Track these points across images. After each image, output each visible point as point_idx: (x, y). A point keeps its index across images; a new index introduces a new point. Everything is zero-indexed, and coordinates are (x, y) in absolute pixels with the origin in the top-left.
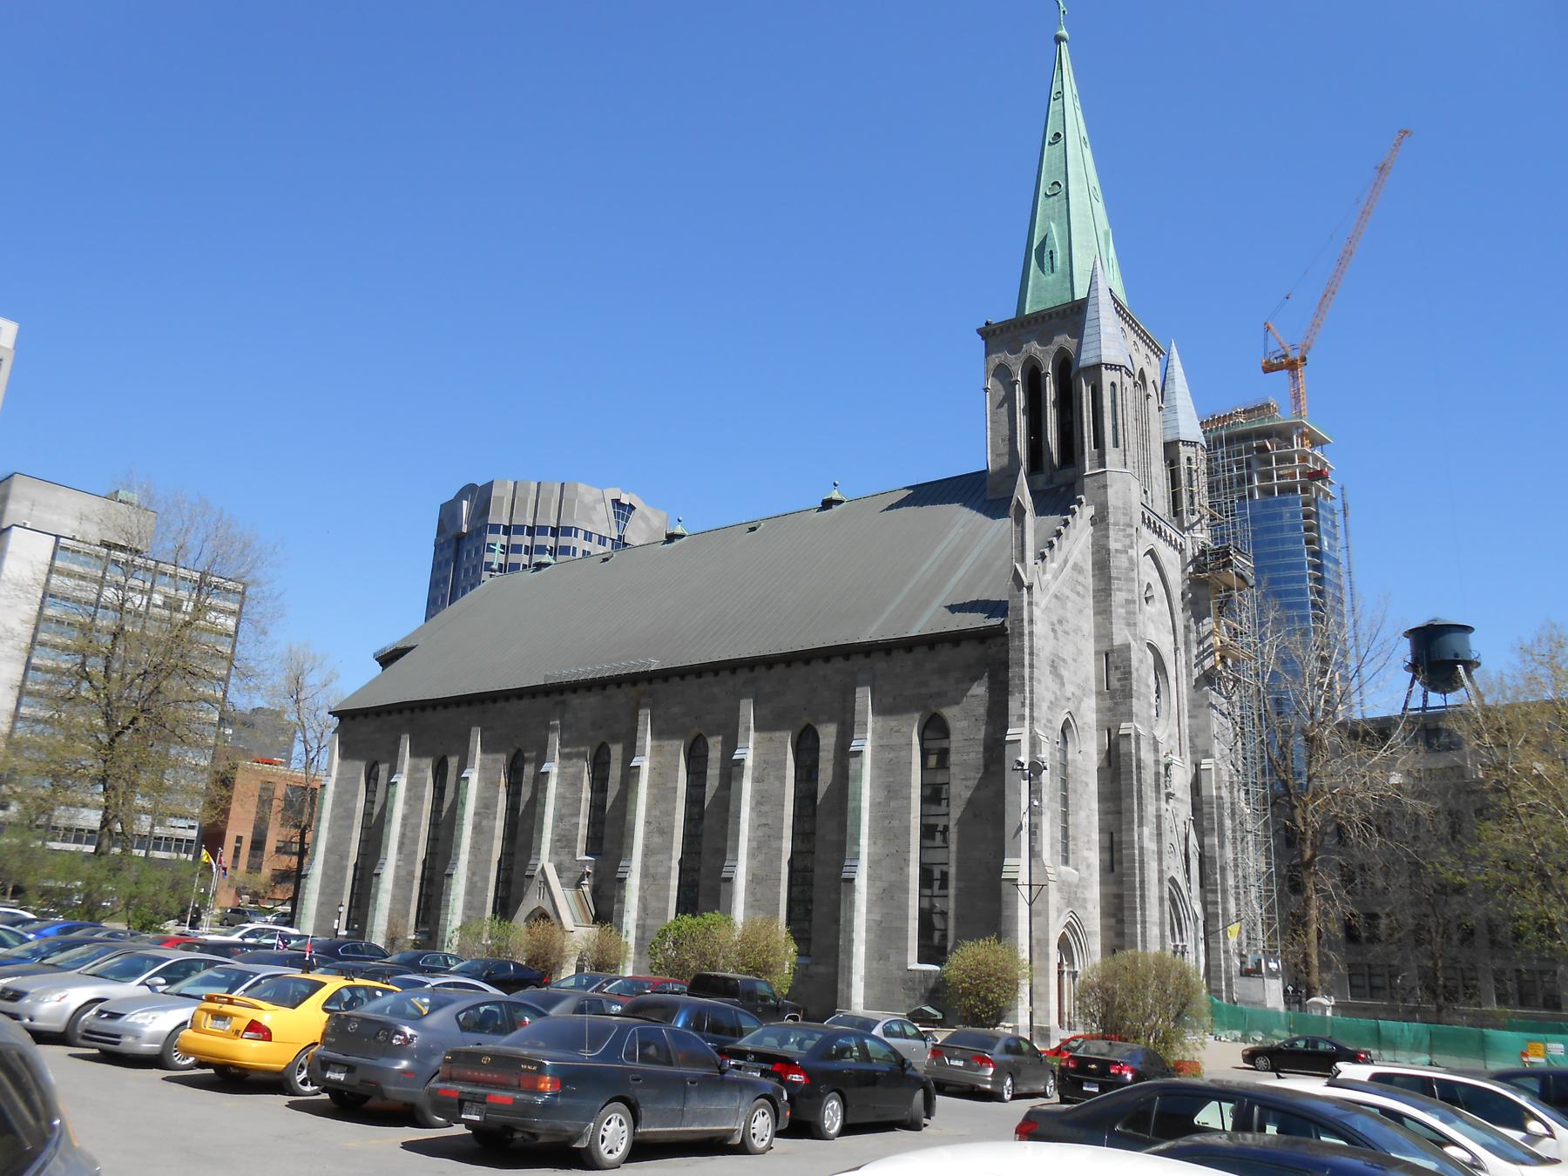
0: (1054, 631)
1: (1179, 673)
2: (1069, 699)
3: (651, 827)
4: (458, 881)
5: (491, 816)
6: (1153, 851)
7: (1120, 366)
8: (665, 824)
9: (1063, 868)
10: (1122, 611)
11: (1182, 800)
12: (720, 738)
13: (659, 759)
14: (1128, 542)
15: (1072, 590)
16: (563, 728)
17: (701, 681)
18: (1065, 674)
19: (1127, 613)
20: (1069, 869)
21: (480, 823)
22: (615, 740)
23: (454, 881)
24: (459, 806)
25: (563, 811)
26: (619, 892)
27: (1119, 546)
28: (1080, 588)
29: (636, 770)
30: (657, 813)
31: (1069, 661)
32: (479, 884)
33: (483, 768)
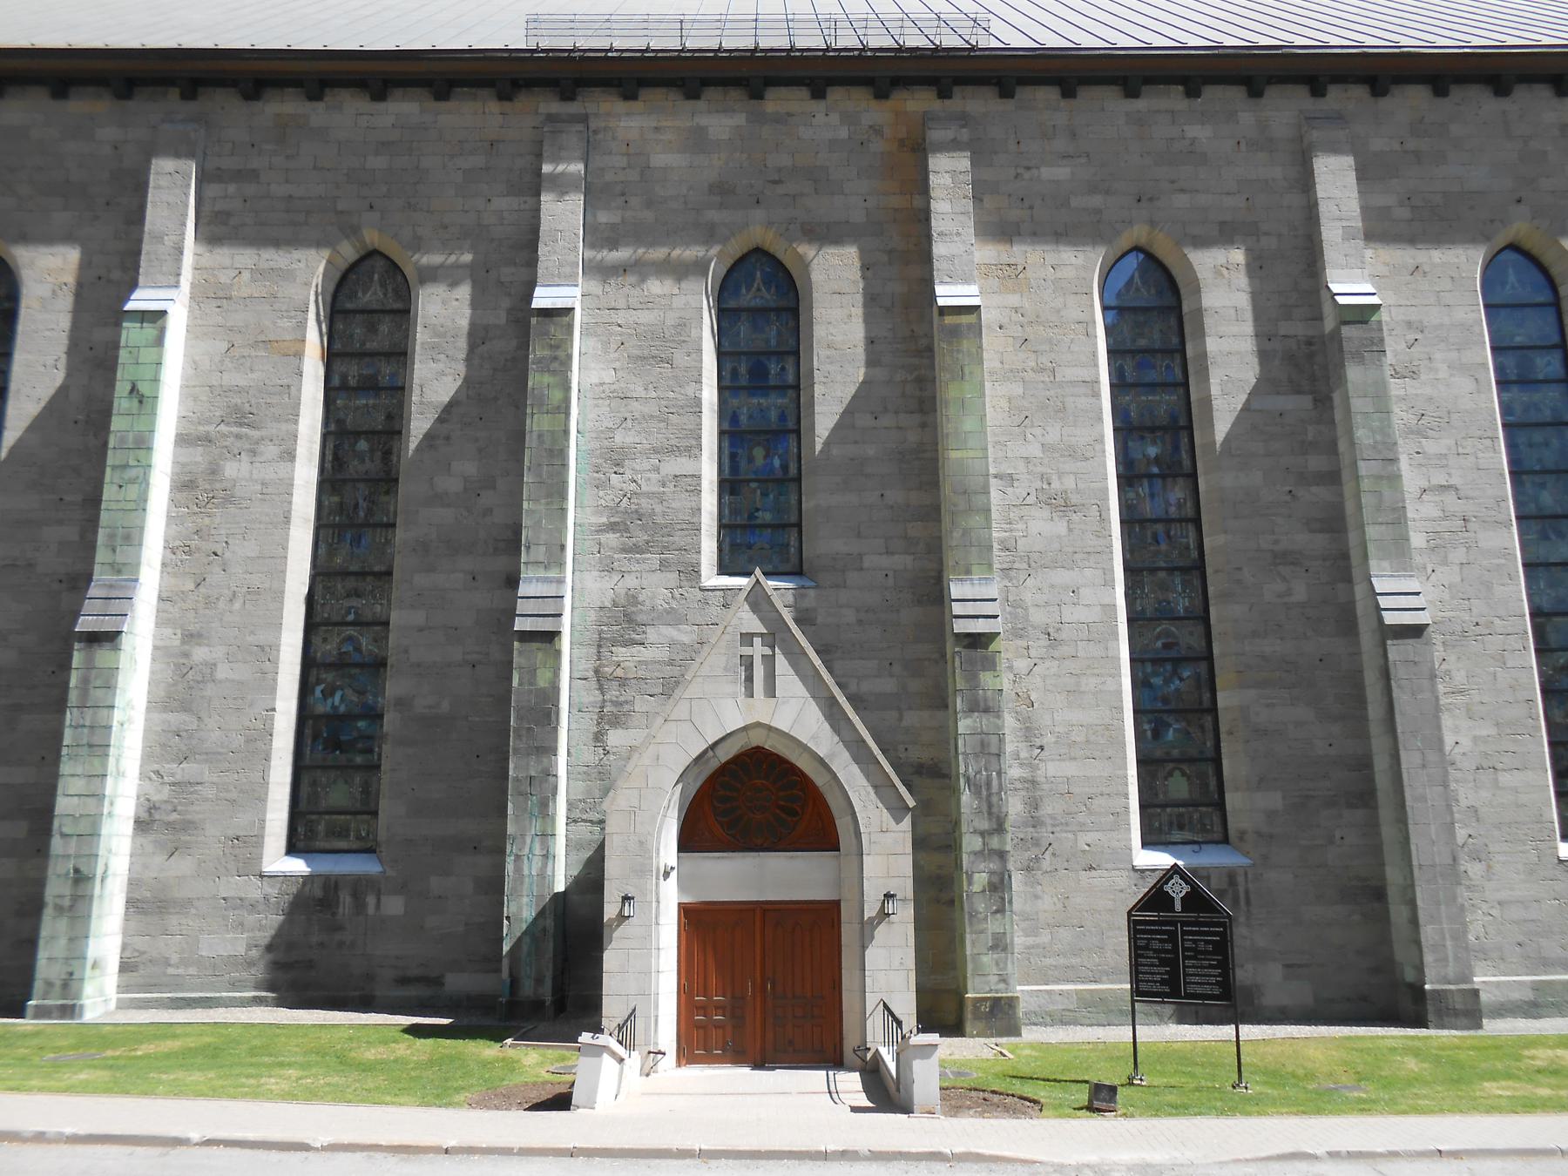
3: (1020, 490)
4: (133, 660)
5: (271, 451)
8: (1069, 483)
12: (1238, 256)
13: (1014, 300)
16: (594, 194)
17: (1140, 104)
21: (214, 471)
22: (827, 234)
23: (124, 659)
24: (122, 401)
25: (619, 438)
26: (972, 678)
29: (965, 319)
30: (1035, 450)
32: (222, 672)
33: (209, 294)
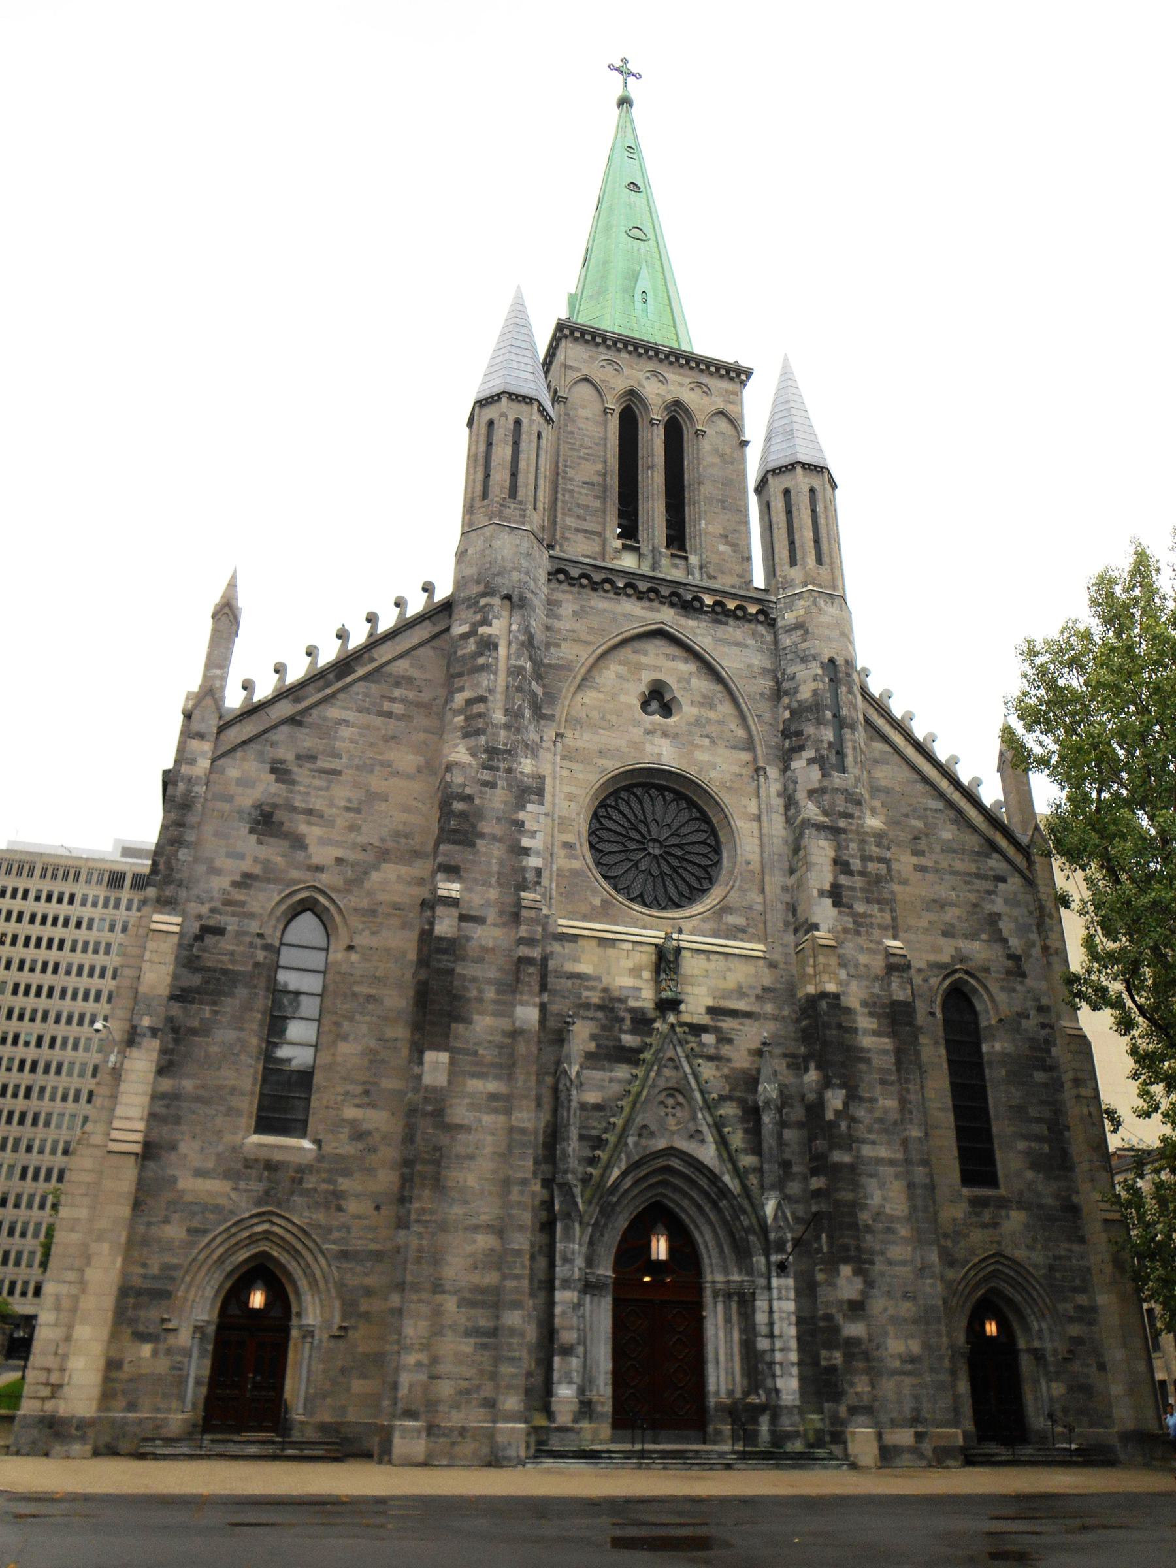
0: (273, 770)
1: (763, 806)
2: (319, 869)
6: (493, 1097)
7: (499, 395)
9: (256, 1138)
10: (460, 719)
11: (748, 1015)
14: (478, 617)
15: (360, 712)
18: (312, 832)
19: (467, 719)
20: (306, 1144)
27: (465, 628)
28: (398, 708)
31: (328, 812)
